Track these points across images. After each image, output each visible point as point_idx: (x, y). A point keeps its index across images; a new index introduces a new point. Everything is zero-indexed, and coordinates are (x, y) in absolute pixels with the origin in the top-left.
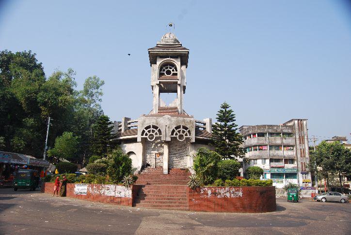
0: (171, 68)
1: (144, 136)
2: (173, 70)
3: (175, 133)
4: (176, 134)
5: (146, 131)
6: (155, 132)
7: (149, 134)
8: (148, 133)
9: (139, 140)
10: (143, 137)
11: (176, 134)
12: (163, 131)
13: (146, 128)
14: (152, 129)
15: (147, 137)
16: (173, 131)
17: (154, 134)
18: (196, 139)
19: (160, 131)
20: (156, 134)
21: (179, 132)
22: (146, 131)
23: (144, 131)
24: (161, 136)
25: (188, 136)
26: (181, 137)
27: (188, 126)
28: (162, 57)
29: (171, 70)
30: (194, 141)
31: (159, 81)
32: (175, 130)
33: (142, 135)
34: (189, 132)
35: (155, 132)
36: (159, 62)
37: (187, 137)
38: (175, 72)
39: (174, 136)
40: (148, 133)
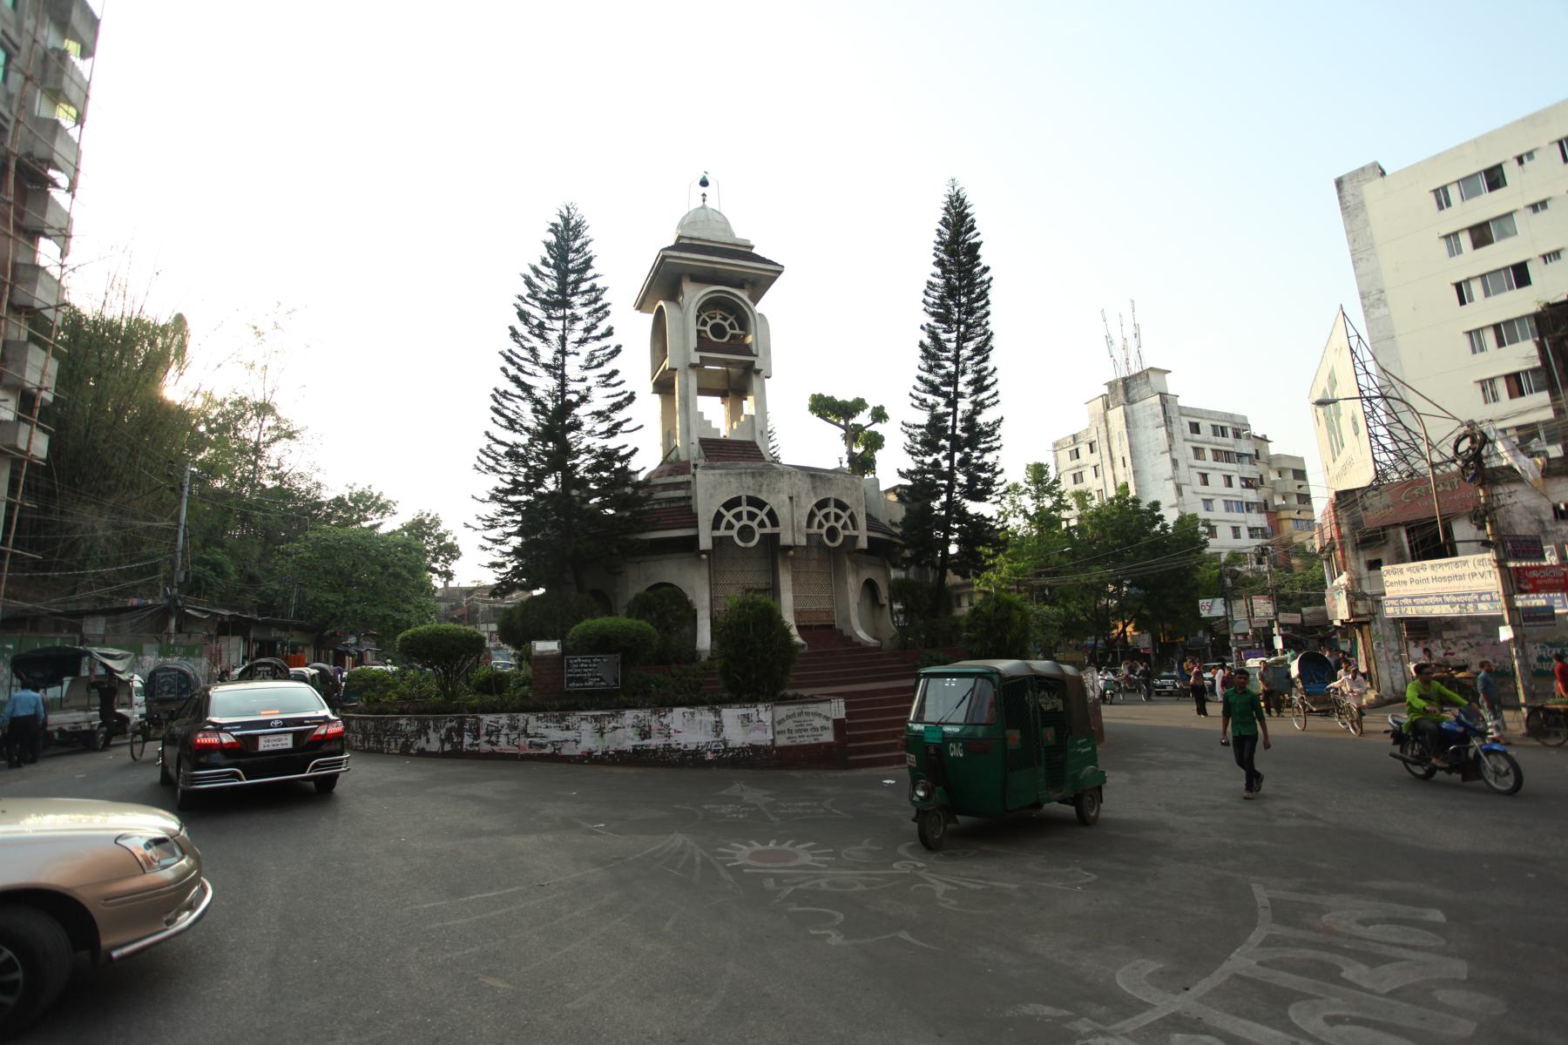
0: (725, 319)
1: (722, 532)
2: (732, 326)
3: (816, 520)
4: (820, 525)
5: (729, 516)
6: (758, 520)
7: (737, 525)
8: (733, 521)
9: (705, 543)
10: (717, 533)
11: (820, 525)
12: (783, 513)
13: (730, 504)
14: (744, 509)
15: (734, 533)
16: (812, 515)
17: (754, 524)
18: (870, 539)
19: (772, 515)
20: (762, 524)
21: (826, 516)
22: (729, 516)
23: (718, 517)
24: (776, 530)
25: (850, 532)
26: (832, 533)
27: (845, 500)
28: (701, 277)
29: (726, 324)
30: (863, 543)
31: (699, 354)
32: (816, 511)
33: (716, 526)
34: (852, 517)
35: (758, 520)
36: (694, 295)
37: (847, 533)
38: (737, 331)
39: (814, 530)
40: (733, 521)
